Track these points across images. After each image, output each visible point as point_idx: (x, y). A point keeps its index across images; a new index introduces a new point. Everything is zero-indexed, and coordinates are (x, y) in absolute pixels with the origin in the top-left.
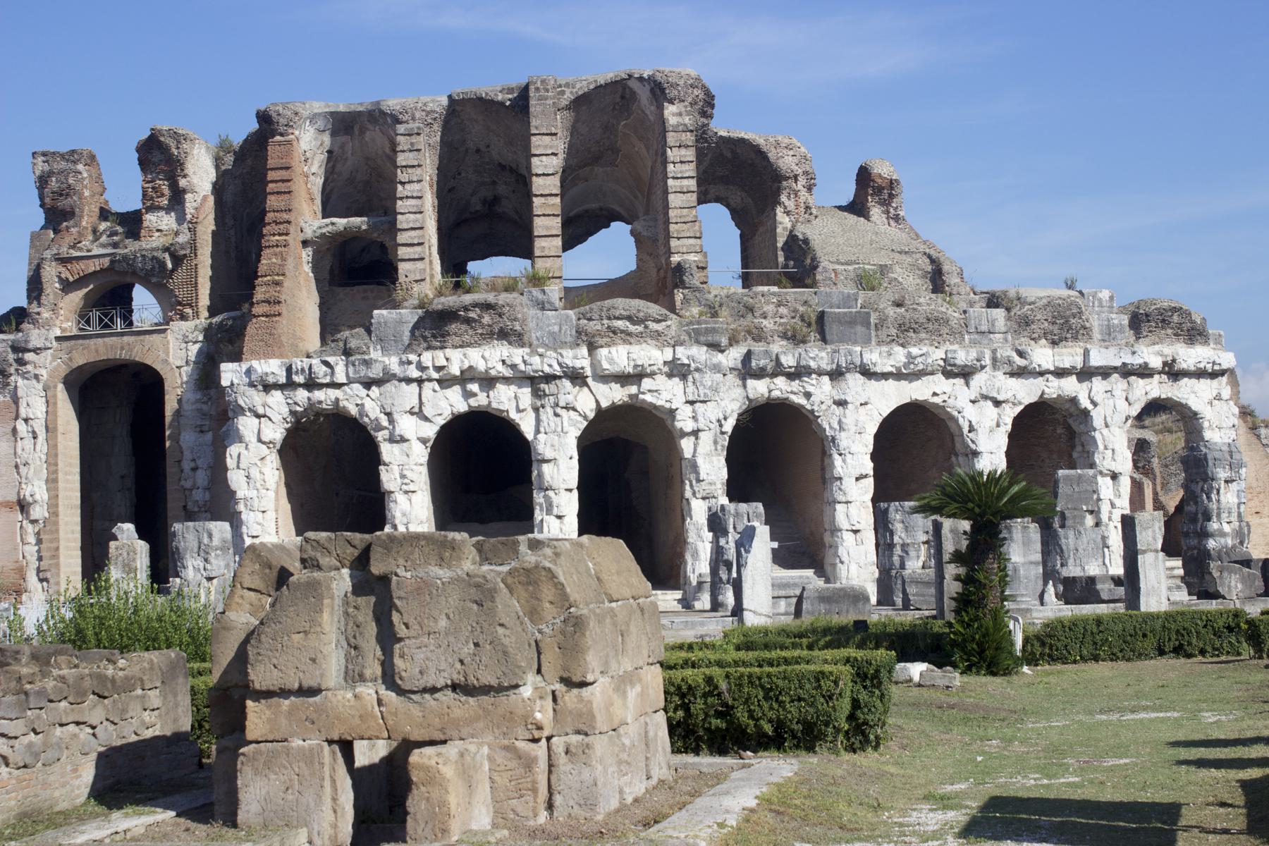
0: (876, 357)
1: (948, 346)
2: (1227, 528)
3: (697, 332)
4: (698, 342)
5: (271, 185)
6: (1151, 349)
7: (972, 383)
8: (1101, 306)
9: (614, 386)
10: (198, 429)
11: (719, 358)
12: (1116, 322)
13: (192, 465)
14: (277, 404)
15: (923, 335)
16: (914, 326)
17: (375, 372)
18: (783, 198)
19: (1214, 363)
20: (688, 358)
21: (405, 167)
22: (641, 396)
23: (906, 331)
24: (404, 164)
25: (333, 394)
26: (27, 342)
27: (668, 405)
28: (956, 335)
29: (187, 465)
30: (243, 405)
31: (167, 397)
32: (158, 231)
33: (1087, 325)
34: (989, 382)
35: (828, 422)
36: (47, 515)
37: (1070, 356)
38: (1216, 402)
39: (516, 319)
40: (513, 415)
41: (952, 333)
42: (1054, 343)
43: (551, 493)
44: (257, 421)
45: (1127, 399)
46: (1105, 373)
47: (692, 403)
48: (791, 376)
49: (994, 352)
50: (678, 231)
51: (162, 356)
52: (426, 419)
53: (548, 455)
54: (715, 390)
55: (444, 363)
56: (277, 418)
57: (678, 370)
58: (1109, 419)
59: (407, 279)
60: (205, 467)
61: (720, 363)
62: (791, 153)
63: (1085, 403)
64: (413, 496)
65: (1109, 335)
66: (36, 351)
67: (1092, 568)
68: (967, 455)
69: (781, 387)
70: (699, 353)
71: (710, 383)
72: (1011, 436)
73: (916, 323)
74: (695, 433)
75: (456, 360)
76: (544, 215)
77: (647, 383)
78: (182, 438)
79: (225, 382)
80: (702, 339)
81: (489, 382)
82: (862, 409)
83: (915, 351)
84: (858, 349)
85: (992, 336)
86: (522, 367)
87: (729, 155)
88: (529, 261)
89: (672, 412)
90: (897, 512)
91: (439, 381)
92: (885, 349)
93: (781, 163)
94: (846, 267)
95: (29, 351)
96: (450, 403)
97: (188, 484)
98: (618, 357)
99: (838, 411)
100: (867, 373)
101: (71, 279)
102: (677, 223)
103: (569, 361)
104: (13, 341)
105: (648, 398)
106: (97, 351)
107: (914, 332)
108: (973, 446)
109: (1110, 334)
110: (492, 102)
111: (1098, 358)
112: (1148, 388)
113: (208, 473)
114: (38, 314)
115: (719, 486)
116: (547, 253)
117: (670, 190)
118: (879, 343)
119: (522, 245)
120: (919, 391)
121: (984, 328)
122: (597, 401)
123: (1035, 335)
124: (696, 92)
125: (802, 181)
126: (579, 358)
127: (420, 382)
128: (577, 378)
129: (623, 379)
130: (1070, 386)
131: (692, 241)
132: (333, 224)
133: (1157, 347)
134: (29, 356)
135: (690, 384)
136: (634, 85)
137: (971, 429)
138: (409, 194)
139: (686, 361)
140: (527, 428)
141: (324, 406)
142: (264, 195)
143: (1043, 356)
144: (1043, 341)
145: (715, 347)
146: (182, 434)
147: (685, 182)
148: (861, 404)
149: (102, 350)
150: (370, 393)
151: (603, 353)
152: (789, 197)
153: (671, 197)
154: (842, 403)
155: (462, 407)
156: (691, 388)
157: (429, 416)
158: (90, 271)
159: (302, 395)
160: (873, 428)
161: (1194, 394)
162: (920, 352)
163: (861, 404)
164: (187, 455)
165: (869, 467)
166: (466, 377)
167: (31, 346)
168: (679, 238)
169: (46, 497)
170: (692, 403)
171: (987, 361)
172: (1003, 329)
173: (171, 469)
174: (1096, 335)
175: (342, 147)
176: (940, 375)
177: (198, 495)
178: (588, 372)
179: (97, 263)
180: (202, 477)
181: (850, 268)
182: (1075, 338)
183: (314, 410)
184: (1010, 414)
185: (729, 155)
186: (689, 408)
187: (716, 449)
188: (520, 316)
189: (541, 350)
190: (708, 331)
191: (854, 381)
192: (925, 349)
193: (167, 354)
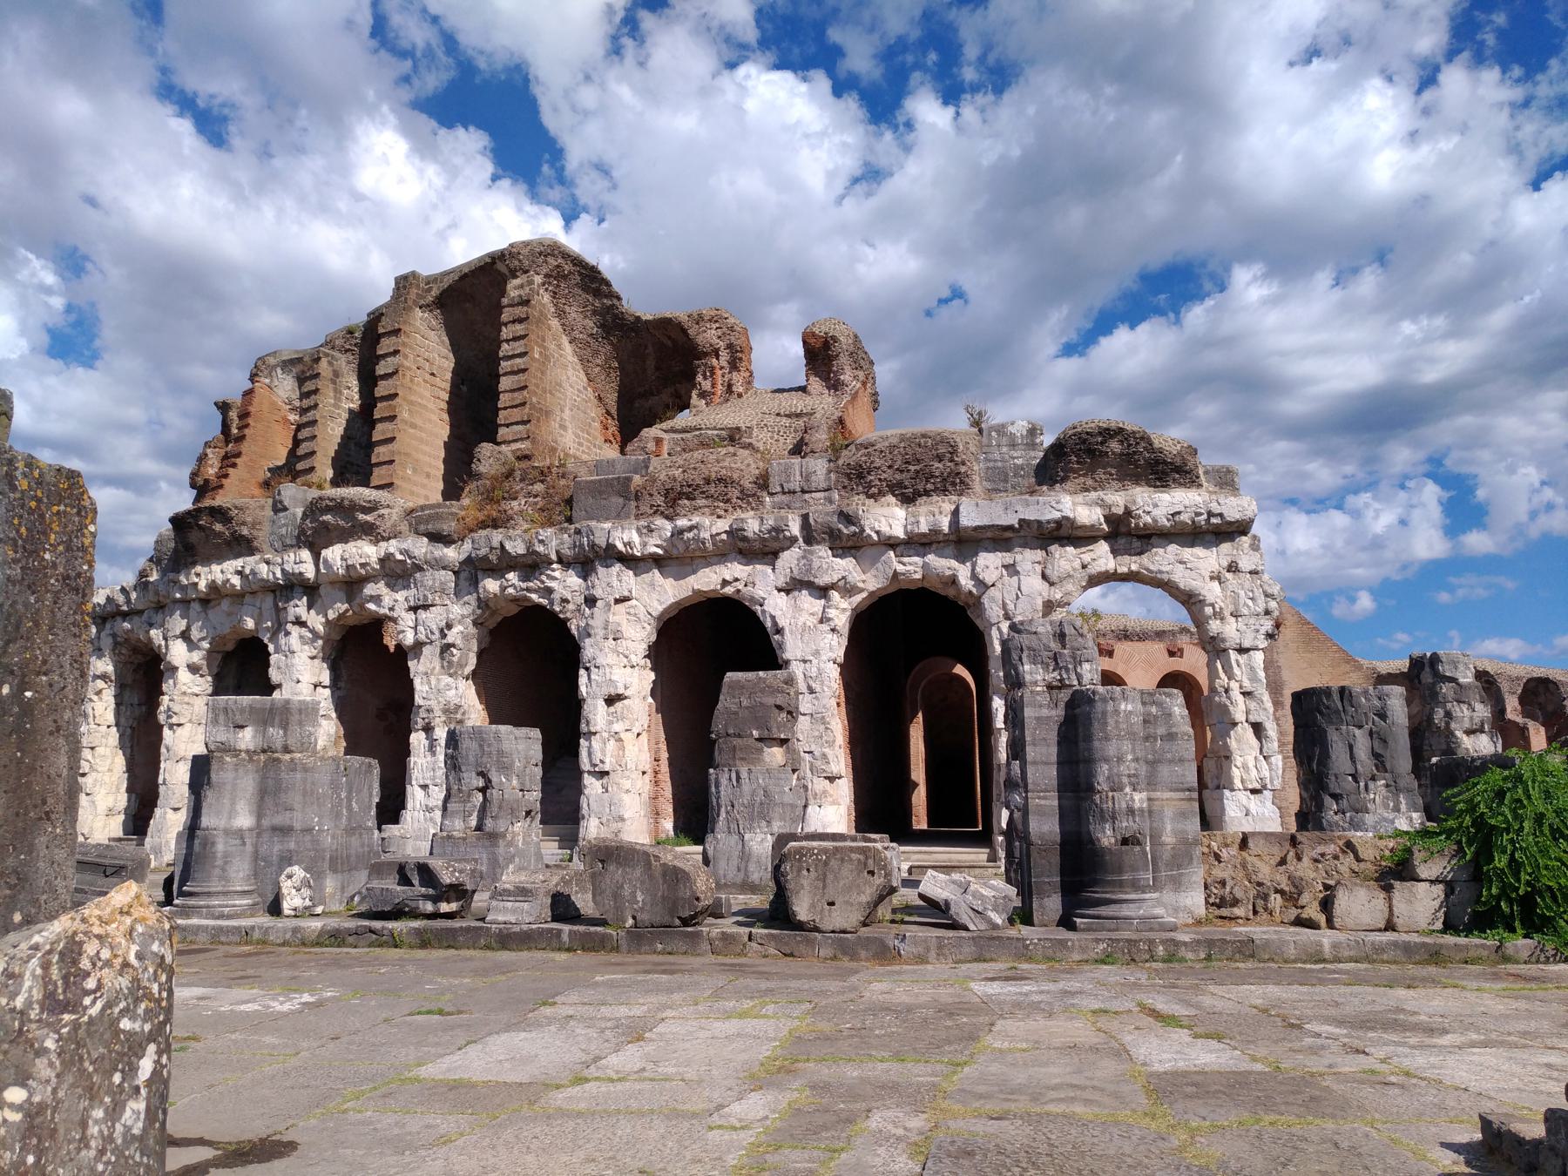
0: (627, 536)
1: (739, 514)
3: (419, 521)
4: (417, 533)
6: (1080, 498)
7: (779, 563)
8: (1013, 445)
12: (1019, 462)
15: (701, 502)
16: (686, 490)
18: (699, 378)
19: (1210, 514)
20: (401, 553)
23: (675, 498)
28: (749, 498)
33: (963, 469)
34: (803, 562)
37: (934, 514)
38: (1229, 576)
39: (244, 523)
41: (745, 495)
42: (907, 500)
45: (1044, 577)
46: (1000, 538)
49: (805, 517)
50: (506, 418)
58: (1011, 606)
61: (445, 556)
62: (714, 326)
63: (966, 582)
64: (179, 731)
65: (1000, 481)
67: (759, 837)
70: (420, 547)
71: (430, 583)
73: (689, 486)
74: (418, 645)
82: (621, 607)
83: (682, 522)
84: (607, 525)
85: (807, 496)
87: (669, 343)
92: (643, 523)
93: (700, 340)
94: (684, 436)
102: (505, 408)
103: (288, 568)
107: (688, 499)
109: (1006, 481)
111: (973, 515)
112: (1087, 558)
115: (438, 713)
117: (501, 372)
118: (637, 517)
120: (707, 580)
121: (795, 484)
123: (874, 490)
124: (552, 262)
125: (724, 356)
128: (310, 590)
131: (520, 427)
133: (1093, 495)
137: (779, 631)
139: (399, 557)
143: (889, 518)
144: (891, 499)
145: (437, 538)
147: (518, 360)
148: (617, 601)
152: (705, 378)
162: (689, 524)
163: (617, 601)
166: (216, 593)
171: (795, 528)
172: (823, 485)
174: (978, 485)
181: (688, 435)
182: (945, 491)
185: (669, 343)
186: (411, 615)
187: (443, 667)
188: (249, 519)
190: (430, 518)
192: (696, 519)
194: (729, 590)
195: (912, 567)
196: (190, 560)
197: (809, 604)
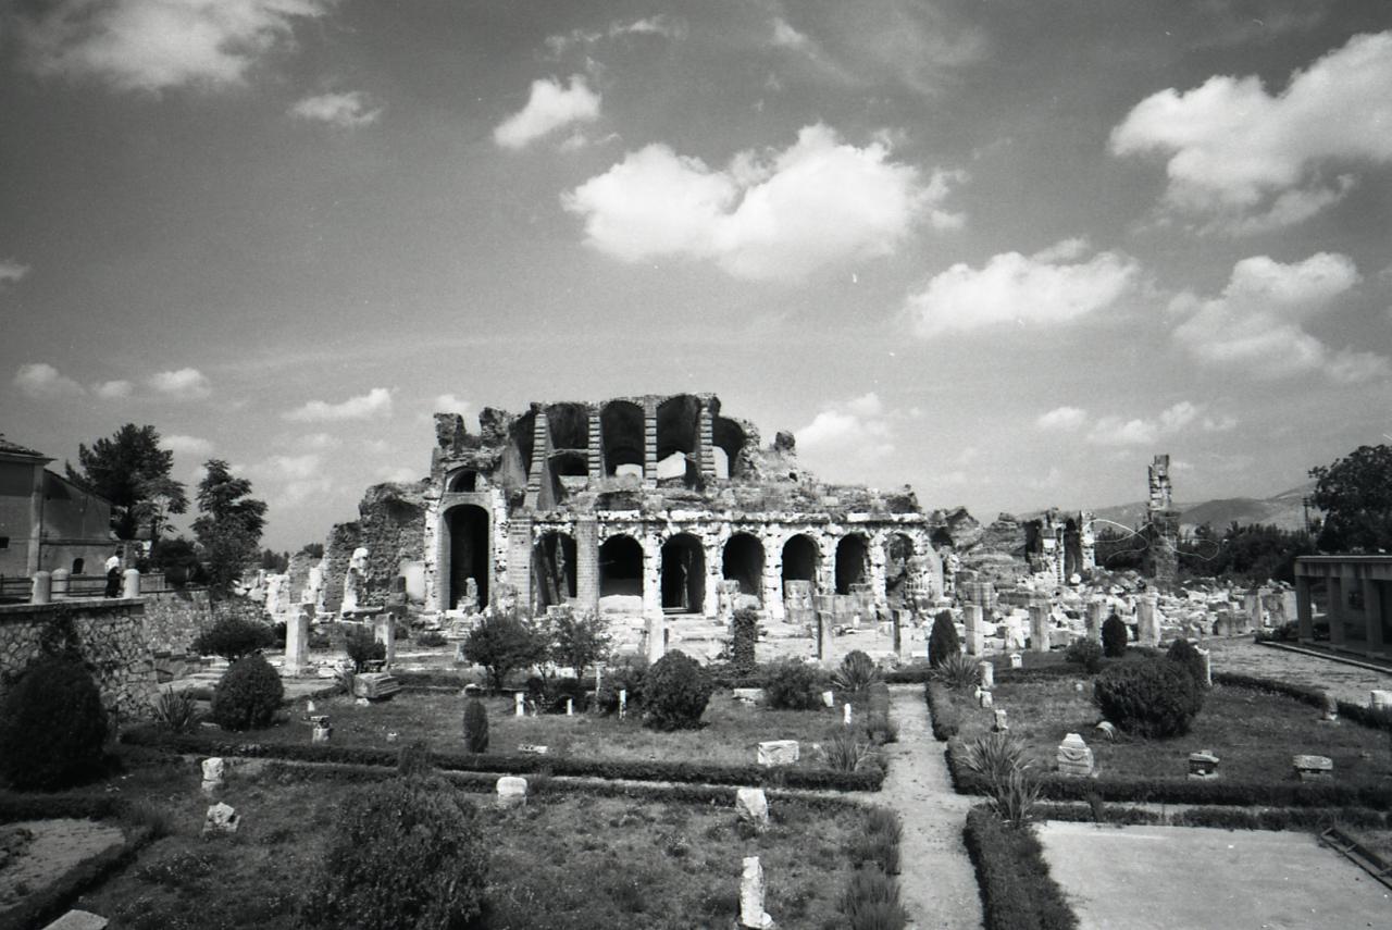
2: (925, 592)
11: (720, 516)
25: (560, 527)
29: (497, 551)
35: (765, 543)
47: (709, 534)
48: (750, 523)
53: (649, 555)
54: (719, 529)
57: (703, 522)
63: (867, 535)
66: (435, 499)
69: (746, 529)
72: (837, 549)
75: (613, 515)
81: (626, 524)
88: (640, 468)
89: (701, 538)
90: (793, 585)
91: (605, 523)
98: (679, 515)
100: (781, 523)
105: (691, 532)
119: (639, 459)
129: (680, 523)
130: (863, 530)
140: (642, 542)
142: (533, 439)
151: (673, 513)
154: (769, 535)
159: (548, 527)
160: (782, 546)
161: (912, 534)
164: (497, 547)
165: (780, 562)
170: (709, 534)
173: (491, 552)
178: (668, 520)
184: (837, 540)
191: (775, 528)
195: (854, 530)
197: (829, 538)
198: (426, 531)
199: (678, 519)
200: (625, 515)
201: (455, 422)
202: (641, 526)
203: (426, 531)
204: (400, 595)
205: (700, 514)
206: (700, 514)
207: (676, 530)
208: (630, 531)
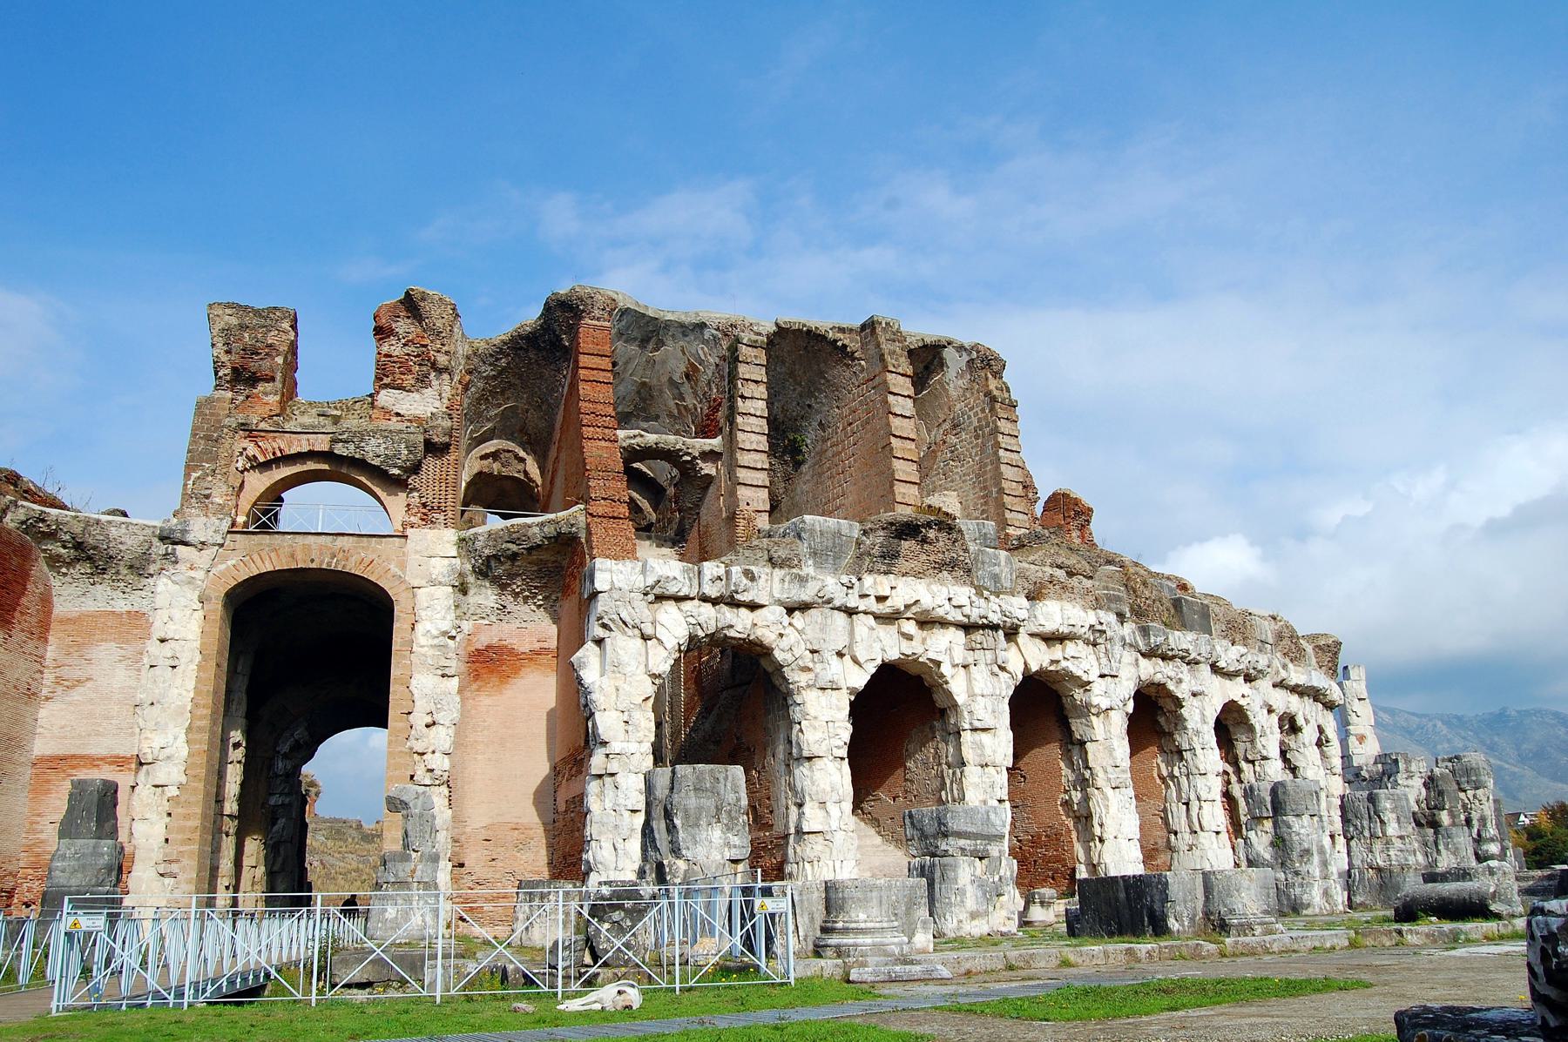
5: (581, 371)
9: (1043, 645)
10: (440, 672)
13: (429, 720)
14: (674, 625)
17: (806, 595)
21: (747, 380)
22: (1064, 664)
24: (747, 377)
26: (184, 532)
27: (1085, 678)
29: (420, 719)
30: (627, 619)
31: (396, 625)
32: (398, 414)
36: (183, 779)
40: (946, 669)
43: (991, 770)
44: (640, 641)
47: (1102, 676)
51: (394, 569)
52: (855, 661)
55: (886, 592)
56: (671, 643)
57: (1096, 637)
59: (747, 507)
60: (447, 723)
68: (1253, 762)
75: (906, 590)
76: (903, 459)
77: (1071, 648)
78: (414, 682)
79: (601, 583)
80: (1113, 606)
81: (927, 622)
86: (967, 610)
95: (186, 544)
96: (884, 646)
97: (419, 747)
98: (1055, 613)
99: (1195, 701)
101: (261, 459)
104: (162, 530)
106: (292, 556)
108: (1265, 753)
110: (823, 338)
113: (451, 731)
114: (207, 497)
116: (906, 500)
122: (1026, 664)
126: (1017, 606)
127: (850, 612)
129: (1052, 639)
132: (642, 436)
134: (179, 548)
135: (1102, 655)
136: (949, 354)
138: (752, 412)
140: (958, 687)
141: (732, 633)
146: (416, 676)
149: (299, 556)
150: (795, 621)
153: (1003, 467)
155: (893, 655)
156: (1104, 661)
157: (862, 660)
158: (292, 452)
167: (190, 538)
168: (1011, 511)
169: (185, 752)
175: (626, 363)
176: (1241, 679)
177: (440, 763)
179: (304, 443)
180: (442, 737)
183: (718, 641)
189: (986, 593)
193: (403, 566)
194: (1242, 702)
196: (883, 568)
198: (153, 647)
199: (1050, 627)
200: (935, 594)
201: (286, 325)
202: (961, 634)
203: (153, 647)
204: (106, 846)
205: (1091, 618)
206: (1091, 618)
207: (1038, 657)
208: (943, 647)
